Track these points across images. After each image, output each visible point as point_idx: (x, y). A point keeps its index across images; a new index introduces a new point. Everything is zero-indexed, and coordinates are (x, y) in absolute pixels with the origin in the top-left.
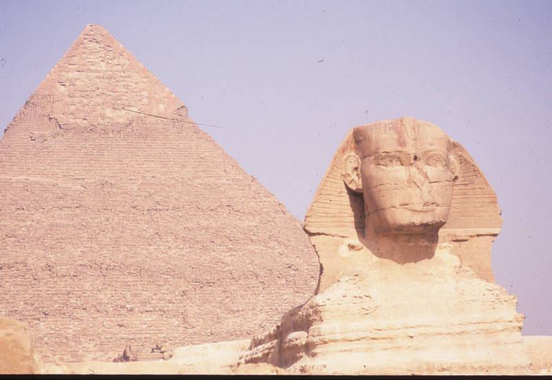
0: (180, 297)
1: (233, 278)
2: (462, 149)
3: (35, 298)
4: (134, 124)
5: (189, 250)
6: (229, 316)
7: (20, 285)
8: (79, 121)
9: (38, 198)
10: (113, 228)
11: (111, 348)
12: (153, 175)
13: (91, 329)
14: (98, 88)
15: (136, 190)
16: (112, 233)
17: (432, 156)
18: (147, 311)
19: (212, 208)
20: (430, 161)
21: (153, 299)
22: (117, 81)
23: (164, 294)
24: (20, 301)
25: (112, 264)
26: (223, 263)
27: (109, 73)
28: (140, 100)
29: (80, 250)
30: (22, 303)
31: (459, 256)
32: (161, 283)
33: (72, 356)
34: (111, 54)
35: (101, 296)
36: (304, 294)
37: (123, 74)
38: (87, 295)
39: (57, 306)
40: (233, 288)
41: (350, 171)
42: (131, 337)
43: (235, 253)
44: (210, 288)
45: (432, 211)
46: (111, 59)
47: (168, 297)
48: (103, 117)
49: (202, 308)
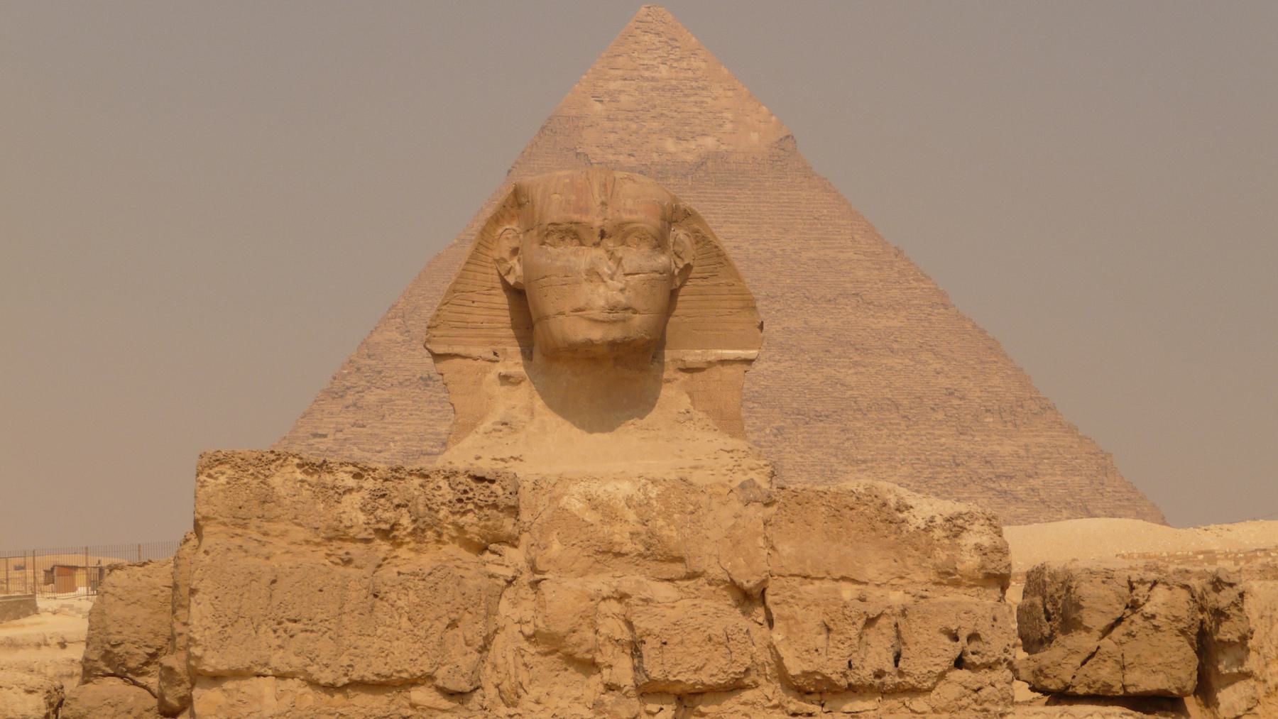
0: (772, 438)
1: (859, 410)
2: (699, 219)
4: (710, 164)
6: (850, 468)
8: (622, 158)
17: (637, 229)
20: (628, 240)
22: (686, 95)
26: (843, 385)
27: (674, 82)
31: (691, 395)
34: (678, 53)
37: (694, 84)
40: (859, 425)
41: (506, 255)
43: (862, 369)
44: (821, 424)
45: (624, 321)
46: (676, 60)
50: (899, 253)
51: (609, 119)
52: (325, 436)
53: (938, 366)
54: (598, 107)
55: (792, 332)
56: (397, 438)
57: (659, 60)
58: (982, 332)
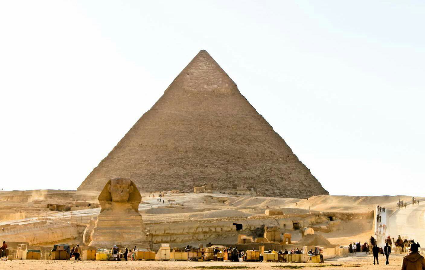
3: (169, 160)
4: (215, 91)
5: (232, 144)
6: (245, 171)
7: (164, 154)
8: (193, 89)
9: (174, 120)
10: (202, 133)
11: (197, 181)
12: (221, 113)
13: (190, 173)
14: (202, 76)
15: (213, 118)
16: (202, 136)
18: (212, 167)
19: (243, 127)
21: (215, 163)
23: (220, 161)
24: (164, 160)
25: (201, 148)
27: (207, 70)
28: (218, 82)
29: (188, 141)
30: (164, 161)
32: (219, 156)
33: (182, 183)
35: (195, 160)
36: (276, 164)
37: (213, 71)
38: (190, 159)
39: (177, 163)
42: (205, 177)
43: (250, 146)
44: (239, 159)
46: (208, 65)
47: (222, 162)
48: (203, 88)
49: (235, 167)
50: (261, 116)
51: (191, 79)
52: (115, 158)
53: (269, 146)
54: (188, 76)
55: (233, 136)
56: (133, 159)
57: (204, 64)
58: (281, 137)
